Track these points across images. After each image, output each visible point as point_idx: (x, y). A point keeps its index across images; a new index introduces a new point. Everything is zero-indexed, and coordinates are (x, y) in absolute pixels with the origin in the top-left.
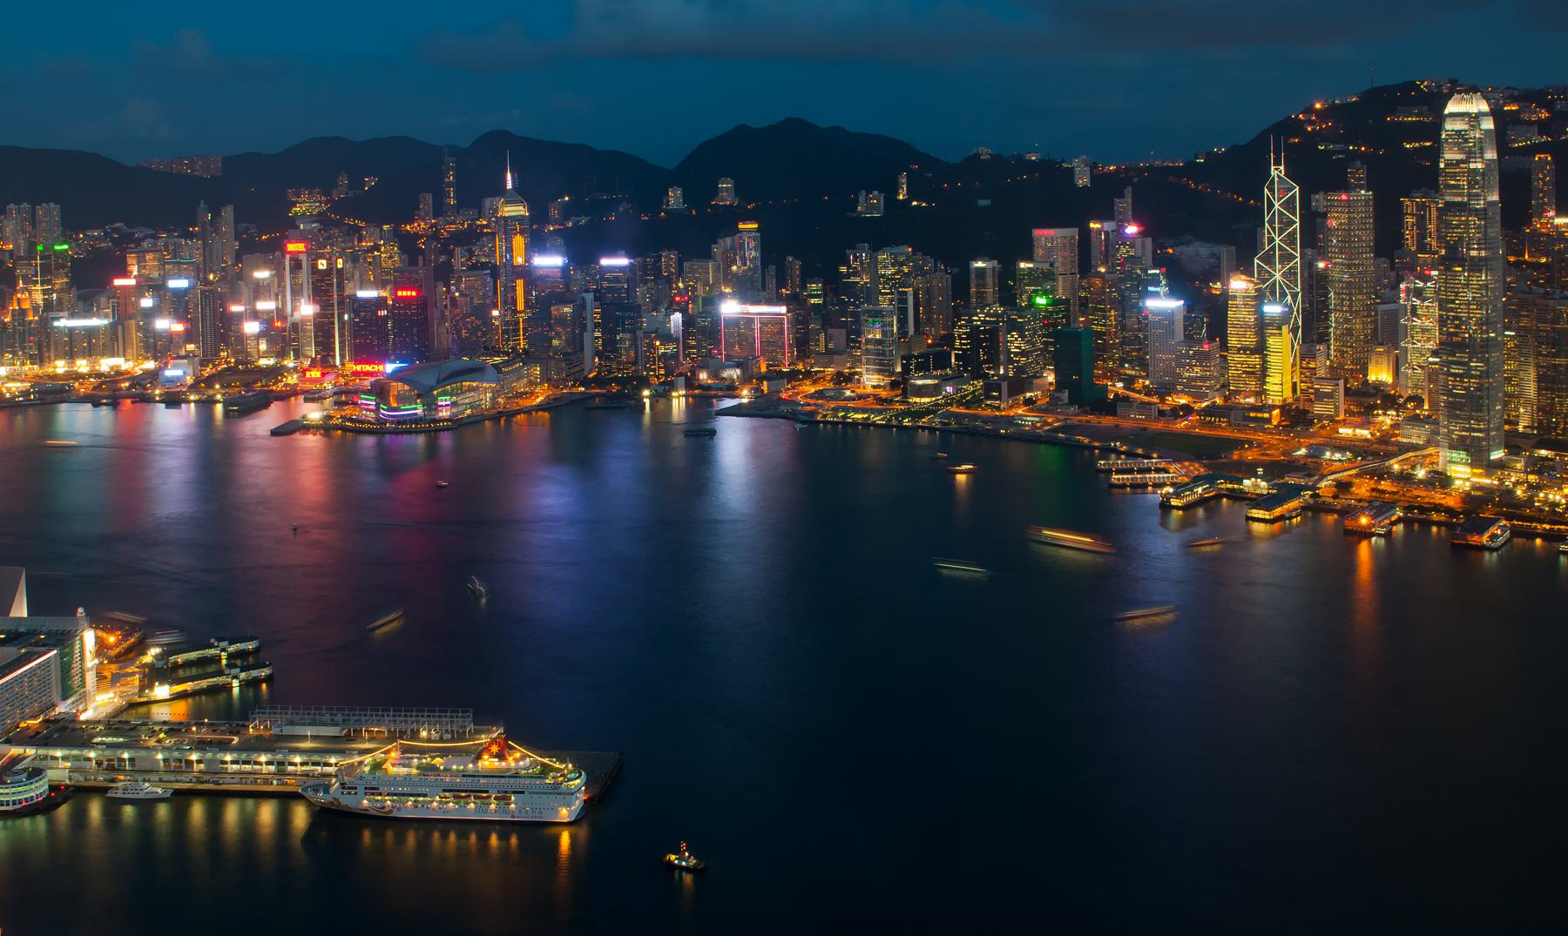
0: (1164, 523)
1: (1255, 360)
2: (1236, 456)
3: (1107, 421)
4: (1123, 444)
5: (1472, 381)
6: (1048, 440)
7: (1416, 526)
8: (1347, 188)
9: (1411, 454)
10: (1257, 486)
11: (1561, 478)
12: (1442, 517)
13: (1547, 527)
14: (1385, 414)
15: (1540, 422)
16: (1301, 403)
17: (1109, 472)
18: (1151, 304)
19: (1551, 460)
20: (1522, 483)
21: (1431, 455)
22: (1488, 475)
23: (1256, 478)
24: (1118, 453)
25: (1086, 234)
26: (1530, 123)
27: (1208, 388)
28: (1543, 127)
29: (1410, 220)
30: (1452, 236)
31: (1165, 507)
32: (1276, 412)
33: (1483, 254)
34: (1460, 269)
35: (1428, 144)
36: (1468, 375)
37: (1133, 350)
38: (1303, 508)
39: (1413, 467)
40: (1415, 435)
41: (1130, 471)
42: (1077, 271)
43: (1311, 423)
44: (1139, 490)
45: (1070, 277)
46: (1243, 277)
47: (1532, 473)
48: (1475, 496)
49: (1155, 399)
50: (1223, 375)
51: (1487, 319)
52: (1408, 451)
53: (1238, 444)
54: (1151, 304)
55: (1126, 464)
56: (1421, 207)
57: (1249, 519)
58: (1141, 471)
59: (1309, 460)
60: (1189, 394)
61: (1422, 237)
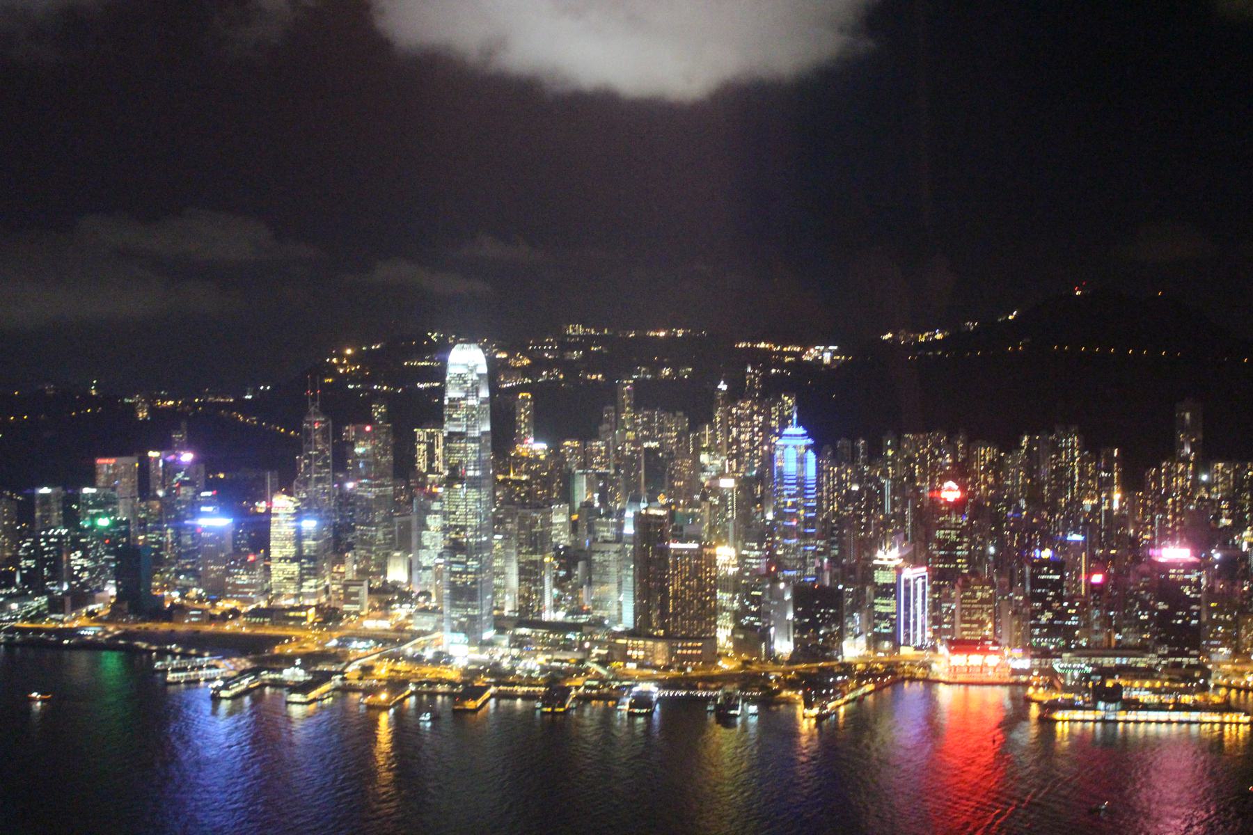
0: (214, 712)
1: (295, 568)
2: (277, 650)
3: (164, 627)
4: (178, 645)
5: (469, 576)
6: (111, 645)
7: (425, 697)
8: (370, 421)
9: (421, 639)
10: (295, 675)
11: (536, 650)
12: (446, 688)
13: (526, 689)
14: (401, 607)
15: (520, 607)
16: (333, 601)
17: (165, 671)
18: (203, 522)
19: (529, 636)
20: (507, 656)
21: (437, 639)
22: (481, 652)
23: (296, 667)
24: (174, 655)
25: (145, 463)
26: (515, 368)
27: (254, 593)
28: (525, 371)
29: (422, 447)
30: (454, 459)
31: (216, 699)
32: (312, 611)
33: (478, 473)
34: (459, 486)
35: (437, 384)
36: (465, 572)
37: (187, 564)
38: (335, 690)
39: (423, 650)
40: (426, 623)
41: (184, 669)
42: (137, 493)
43: (341, 619)
44: (192, 685)
45: (131, 501)
46: (285, 497)
47: (514, 647)
48: (471, 670)
49: (207, 604)
50: (267, 582)
51: (481, 525)
52: (419, 636)
53: (278, 640)
54: (203, 522)
55: (181, 663)
56: (431, 436)
57: (288, 703)
58: (192, 669)
59: (339, 650)
60: (237, 599)
61: (431, 458)
